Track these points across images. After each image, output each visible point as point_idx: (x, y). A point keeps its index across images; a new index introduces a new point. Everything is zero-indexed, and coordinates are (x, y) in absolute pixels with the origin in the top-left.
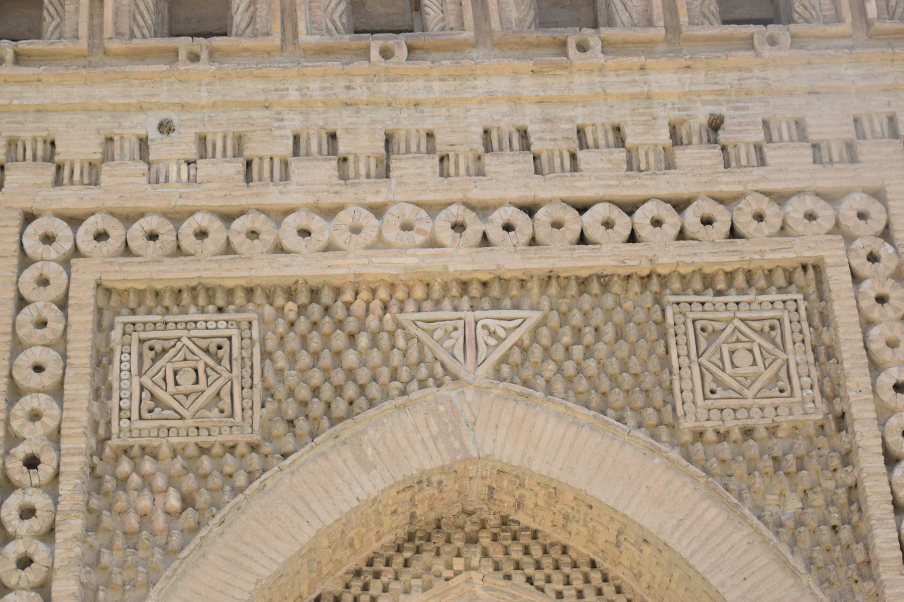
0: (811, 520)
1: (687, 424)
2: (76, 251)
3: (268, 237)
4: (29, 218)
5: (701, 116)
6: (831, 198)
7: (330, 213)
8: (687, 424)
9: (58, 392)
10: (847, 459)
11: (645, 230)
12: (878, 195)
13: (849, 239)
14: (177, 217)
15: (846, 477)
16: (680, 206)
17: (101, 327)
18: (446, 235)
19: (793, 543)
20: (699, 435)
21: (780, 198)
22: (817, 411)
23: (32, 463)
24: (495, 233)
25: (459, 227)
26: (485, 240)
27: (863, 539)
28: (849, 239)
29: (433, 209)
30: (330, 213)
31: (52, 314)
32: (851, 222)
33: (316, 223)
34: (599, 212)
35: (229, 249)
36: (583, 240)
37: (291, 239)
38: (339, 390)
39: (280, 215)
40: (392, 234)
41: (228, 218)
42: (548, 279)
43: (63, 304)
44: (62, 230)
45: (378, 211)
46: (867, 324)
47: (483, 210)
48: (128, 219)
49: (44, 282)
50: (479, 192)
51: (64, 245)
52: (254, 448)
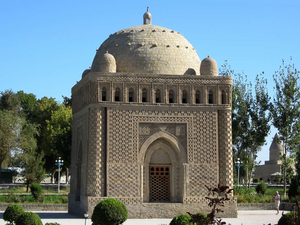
0: (183, 142)
1: (177, 135)
2: (137, 120)
3: (150, 119)
4: (134, 117)
5: (180, 111)
6: (188, 118)
8: (177, 135)
9: (136, 131)
10: (186, 138)
11: (175, 120)
12: (191, 118)
13: (189, 122)
14: (144, 117)
15: (186, 139)
16: (178, 118)
17: (139, 125)
18: (162, 120)
19: (182, 144)
20: (177, 136)
21: (185, 118)
22: (185, 135)
23: (135, 136)
24: (165, 120)
25: (163, 119)
26: (164, 120)
27: (187, 144)
28: (189, 122)
29: (161, 118)
30: (154, 117)
31: (136, 125)
32: (189, 120)
33: (153, 118)
34: (172, 118)
35: (147, 120)
36: (171, 121)
37: (152, 119)
38: (154, 131)
39: (151, 117)
40: (158, 120)
41: (147, 117)
42: (168, 123)
43: (136, 124)
44: (136, 118)
45: (157, 118)
46: (189, 128)
47: (164, 118)
48: (141, 117)
49: (135, 122)
50: (164, 116)
51: (136, 120)
52: (149, 135)
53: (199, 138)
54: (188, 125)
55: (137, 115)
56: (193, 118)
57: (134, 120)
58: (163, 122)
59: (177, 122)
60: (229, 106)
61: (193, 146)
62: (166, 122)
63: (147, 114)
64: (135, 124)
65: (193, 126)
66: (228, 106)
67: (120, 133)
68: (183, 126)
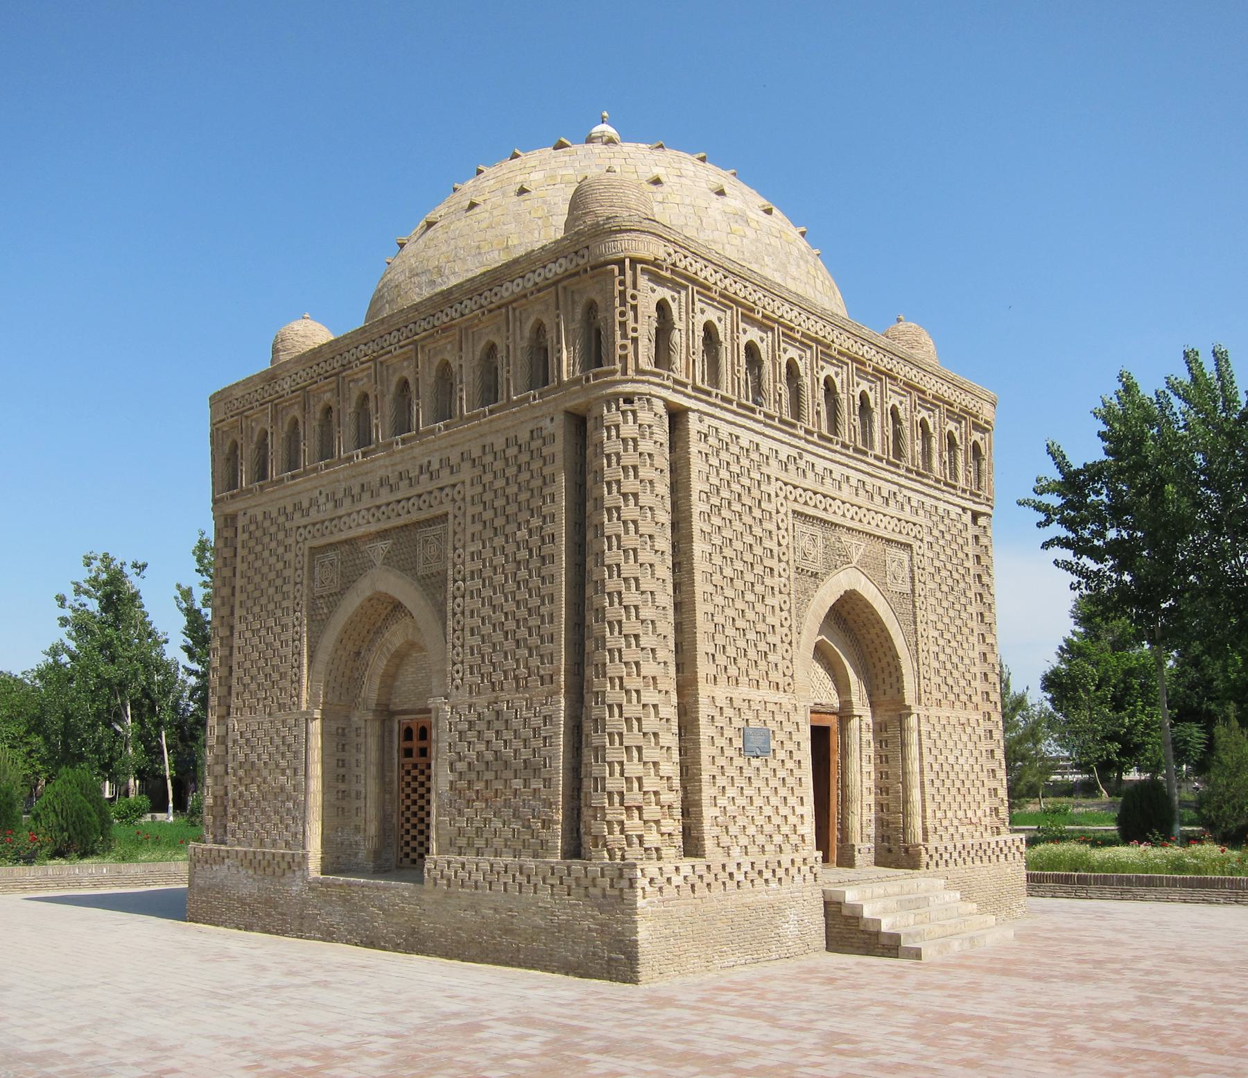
2: (306, 539)
4: (299, 527)
7: (349, 515)
41: (332, 520)
48: (314, 524)
53: (488, 572)
54: (451, 517)
55: (304, 521)
56: (468, 482)
57: (298, 542)
58: (374, 528)
59: (415, 516)
60: (618, 377)
61: (467, 613)
62: (384, 525)
63: (330, 505)
64: (300, 558)
65: (469, 519)
66: (614, 372)
67: (264, 601)
68: (438, 529)
